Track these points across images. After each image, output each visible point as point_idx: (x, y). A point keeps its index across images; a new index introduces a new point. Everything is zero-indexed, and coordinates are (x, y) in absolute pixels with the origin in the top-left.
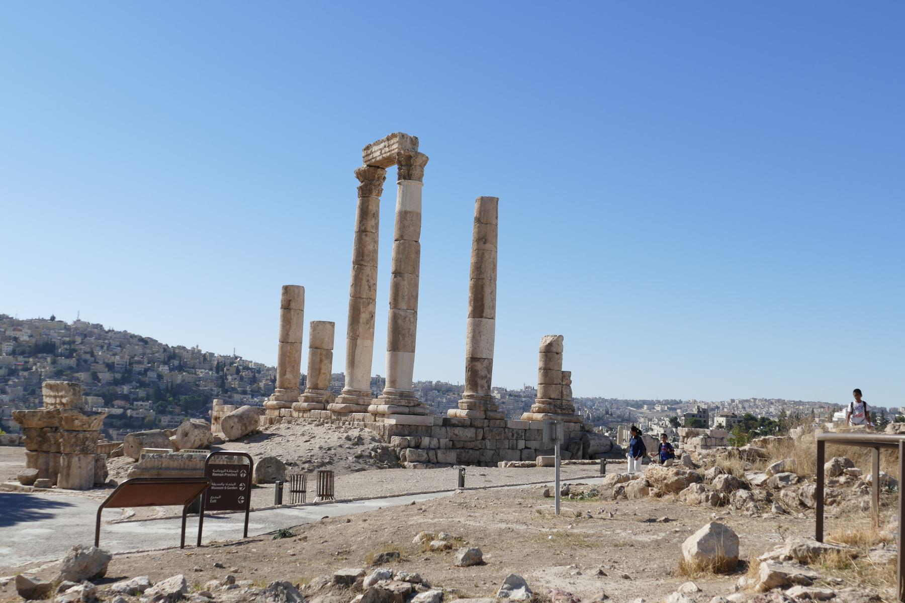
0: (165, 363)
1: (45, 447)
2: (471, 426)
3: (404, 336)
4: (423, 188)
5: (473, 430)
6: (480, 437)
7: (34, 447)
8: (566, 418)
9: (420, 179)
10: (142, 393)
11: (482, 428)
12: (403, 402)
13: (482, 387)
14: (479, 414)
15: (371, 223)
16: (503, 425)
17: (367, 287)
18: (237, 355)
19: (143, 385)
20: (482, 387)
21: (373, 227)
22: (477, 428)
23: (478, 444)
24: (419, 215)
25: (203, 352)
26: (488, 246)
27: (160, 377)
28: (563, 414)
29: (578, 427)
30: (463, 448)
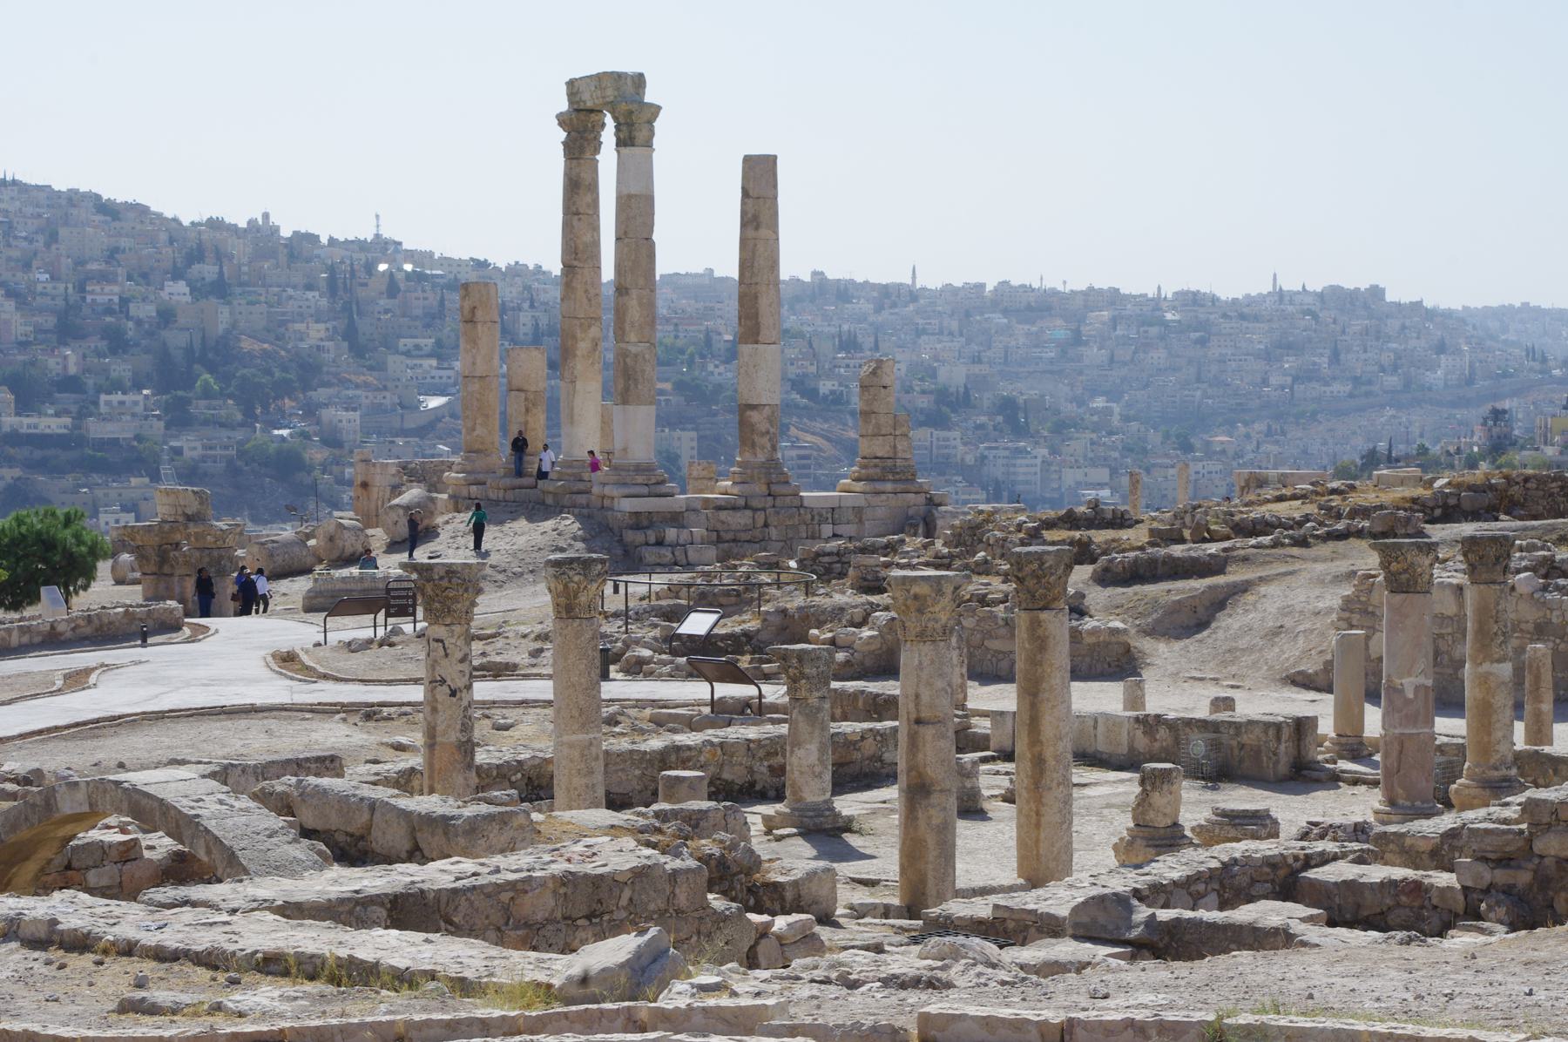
0: (177, 275)
1: (166, 569)
2: (746, 507)
3: (636, 382)
4: (655, 155)
5: (748, 513)
6: (760, 522)
7: (154, 569)
8: (900, 487)
9: (648, 144)
10: (121, 368)
11: (764, 509)
12: (640, 479)
13: (763, 448)
14: (760, 488)
15: (583, 200)
16: (796, 502)
17: (585, 301)
18: (387, 234)
19: (117, 343)
20: (763, 448)
21: (588, 206)
22: (755, 510)
23: (757, 533)
24: (650, 200)
25: (286, 232)
26: (763, 232)
27: (166, 316)
28: (895, 481)
29: (921, 499)
30: (734, 540)
